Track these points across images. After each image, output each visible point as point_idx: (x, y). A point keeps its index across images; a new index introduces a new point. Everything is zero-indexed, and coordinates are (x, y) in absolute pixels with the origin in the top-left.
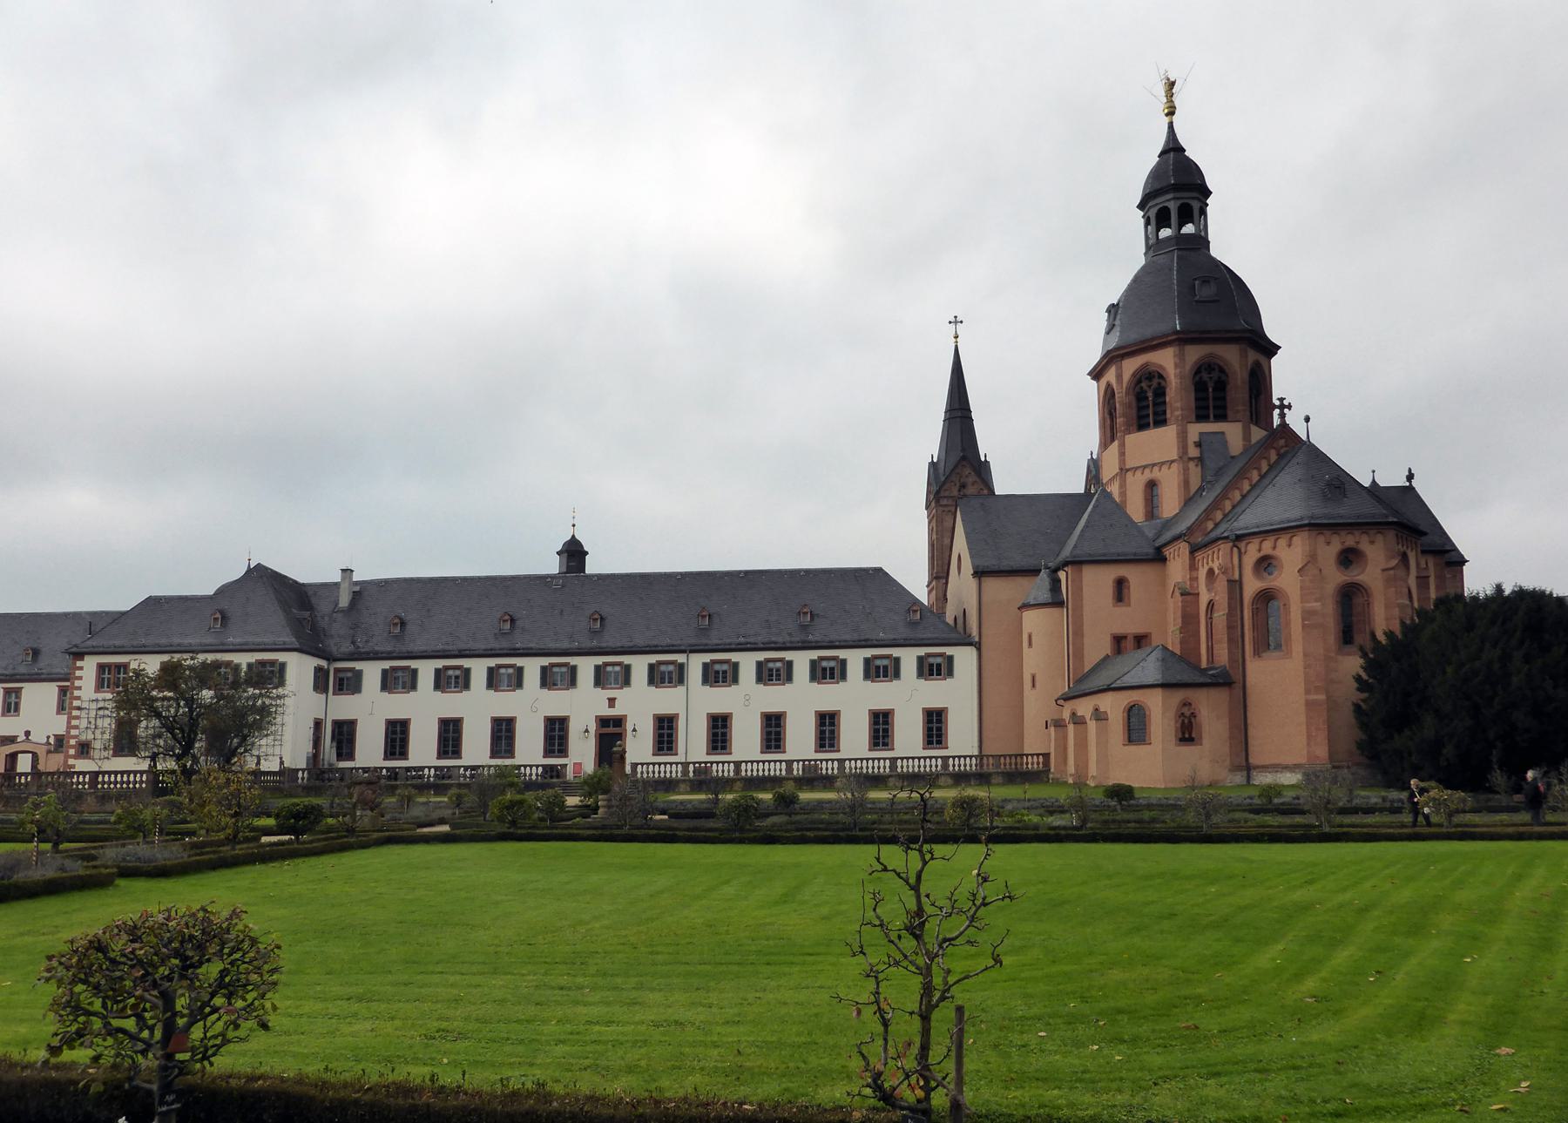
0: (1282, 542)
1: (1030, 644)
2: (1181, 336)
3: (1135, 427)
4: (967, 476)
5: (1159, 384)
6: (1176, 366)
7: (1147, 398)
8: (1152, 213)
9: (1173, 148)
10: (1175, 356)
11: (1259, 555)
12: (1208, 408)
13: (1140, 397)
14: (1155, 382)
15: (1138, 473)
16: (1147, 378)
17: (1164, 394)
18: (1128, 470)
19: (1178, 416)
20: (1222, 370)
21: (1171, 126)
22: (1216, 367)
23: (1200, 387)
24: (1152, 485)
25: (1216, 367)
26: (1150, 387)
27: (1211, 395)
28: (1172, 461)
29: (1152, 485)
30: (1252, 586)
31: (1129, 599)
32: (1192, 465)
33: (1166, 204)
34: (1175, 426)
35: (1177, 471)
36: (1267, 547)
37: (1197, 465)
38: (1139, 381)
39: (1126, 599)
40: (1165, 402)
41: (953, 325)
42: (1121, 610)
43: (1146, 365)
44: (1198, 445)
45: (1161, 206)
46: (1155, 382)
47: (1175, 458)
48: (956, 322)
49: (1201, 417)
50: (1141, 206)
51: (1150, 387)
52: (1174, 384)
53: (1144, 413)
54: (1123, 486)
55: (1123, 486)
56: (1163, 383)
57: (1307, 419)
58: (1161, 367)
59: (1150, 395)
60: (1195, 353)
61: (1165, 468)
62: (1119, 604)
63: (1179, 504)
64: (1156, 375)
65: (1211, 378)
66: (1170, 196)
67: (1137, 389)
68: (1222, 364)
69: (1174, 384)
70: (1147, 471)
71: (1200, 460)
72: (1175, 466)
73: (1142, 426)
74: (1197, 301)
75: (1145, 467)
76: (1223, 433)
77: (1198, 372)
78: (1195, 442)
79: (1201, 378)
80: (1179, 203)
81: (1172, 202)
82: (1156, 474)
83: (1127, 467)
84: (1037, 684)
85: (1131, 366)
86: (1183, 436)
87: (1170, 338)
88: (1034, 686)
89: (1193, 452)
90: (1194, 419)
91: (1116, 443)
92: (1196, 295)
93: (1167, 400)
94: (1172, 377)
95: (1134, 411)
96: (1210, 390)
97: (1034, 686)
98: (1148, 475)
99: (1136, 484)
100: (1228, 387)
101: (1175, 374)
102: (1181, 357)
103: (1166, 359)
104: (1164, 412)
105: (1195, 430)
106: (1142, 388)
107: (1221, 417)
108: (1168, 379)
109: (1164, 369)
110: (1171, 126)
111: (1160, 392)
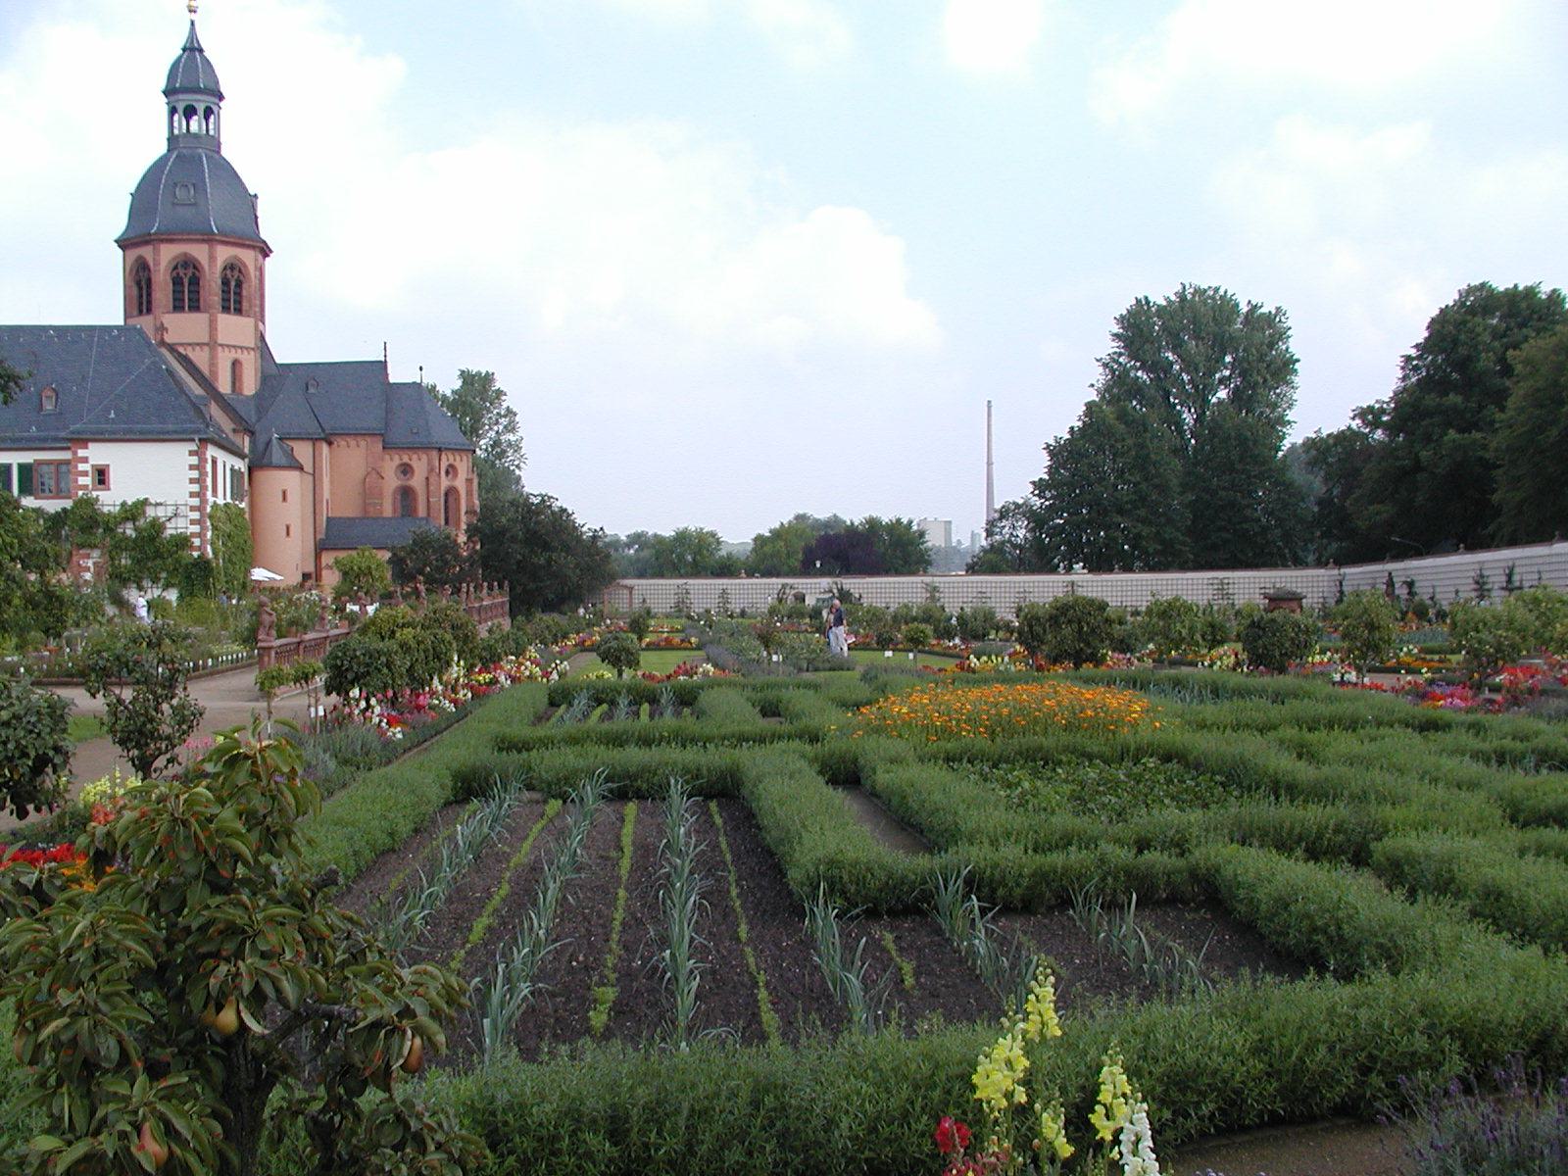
1: (284, 499)
9: (193, 48)
12: (229, 300)
13: (225, 282)
15: (226, 349)
18: (221, 345)
21: (193, 23)
24: (236, 364)
30: (445, 483)
38: (225, 269)
43: (236, 257)
46: (236, 273)
47: (253, 346)
56: (242, 278)
57: (421, 369)
58: (245, 266)
59: (233, 284)
73: (226, 309)
82: (239, 355)
83: (220, 342)
84: (291, 533)
85: (224, 254)
86: (256, 327)
88: (288, 534)
91: (200, 319)
93: (244, 293)
97: (288, 534)
110: (193, 23)
111: (239, 284)
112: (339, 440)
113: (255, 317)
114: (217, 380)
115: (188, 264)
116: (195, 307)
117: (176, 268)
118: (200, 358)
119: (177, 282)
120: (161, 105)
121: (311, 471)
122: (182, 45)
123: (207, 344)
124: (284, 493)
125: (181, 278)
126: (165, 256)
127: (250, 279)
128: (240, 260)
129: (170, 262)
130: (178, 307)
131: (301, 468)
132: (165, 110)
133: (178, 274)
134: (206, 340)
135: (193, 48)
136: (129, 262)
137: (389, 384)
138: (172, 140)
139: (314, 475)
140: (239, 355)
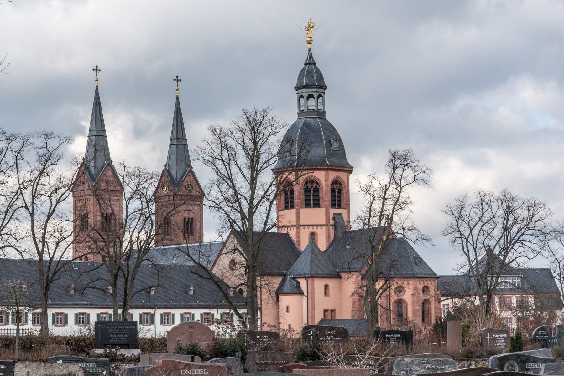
0: (405, 282)
1: (288, 311)
2: (329, 167)
3: (304, 205)
4: (109, 176)
5: (316, 187)
6: (326, 181)
7: (310, 191)
8: (305, 95)
9: (310, 62)
10: (325, 176)
11: (396, 286)
13: (307, 190)
14: (314, 185)
15: (306, 228)
16: (310, 182)
17: (318, 191)
19: (326, 205)
20: (340, 184)
21: (310, 50)
22: (339, 182)
23: (333, 191)
24: (313, 234)
25: (339, 182)
26: (312, 187)
27: (336, 195)
28: (324, 225)
29: (313, 234)
30: (394, 297)
31: (329, 293)
32: (331, 228)
33: (312, 93)
34: (324, 209)
35: (325, 231)
36: (400, 282)
37: (333, 229)
38: (307, 183)
39: (328, 294)
40: (319, 195)
41: (95, 72)
42: (327, 298)
44: (334, 219)
45: (310, 93)
46: (314, 185)
47: (324, 224)
48: (97, 70)
49: (333, 206)
50: (297, 88)
51: (312, 187)
52: (324, 189)
53: (308, 198)
54: (298, 233)
55: (298, 233)
56: (318, 187)
58: (318, 179)
60: (333, 175)
61: (319, 228)
62: (326, 296)
63: (326, 245)
64: (315, 182)
65: (336, 187)
66: (315, 90)
67: (306, 187)
68: (341, 181)
69: (324, 189)
70: (311, 228)
71: (335, 226)
72: (324, 228)
73: (307, 205)
74: (332, 150)
75: (310, 225)
76: (341, 214)
77: (332, 184)
78: (332, 218)
79: (333, 187)
80: (318, 94)
81: (315, 93)
82: (315, 230)
83: (301, 224)
86: (327, 214)
87: (324, 167)
89: (332, 222)
90: (331, 207)
91: (293, 211)
92: (331, 147)
93: (320, 195)
94: (324, 186)
95: (304, 197)
96: (336, 193)
98: (311, 230)
99: (305, 233)
100: (342, 192)
101: (325, 184)
102: (327, 176)
103: (320, 175)
104: (319, 200)
105: (333, 211)
106: (307, 187)
107: (340, 206)
108: (321, 186)
109: (319, 180)
110: (310, 50)
111: (317, 190)
112: (344, 275)
113: (326, 207)
114: (299, 244)
116: (292, 207)
118: (293, 233)
120: (294, 95)
121: (306, 295)
122: (304, 62)
123: (294, 226)
124: (288, 308)
125: (287, 191)
128: (315, 177)
130: (286, 208)
131: (302, 293)
132: (296, 97)
134: (295, 224)
135: (310, 62)
138: (301, 113)
139: (307, 297)
140: (315, 230)
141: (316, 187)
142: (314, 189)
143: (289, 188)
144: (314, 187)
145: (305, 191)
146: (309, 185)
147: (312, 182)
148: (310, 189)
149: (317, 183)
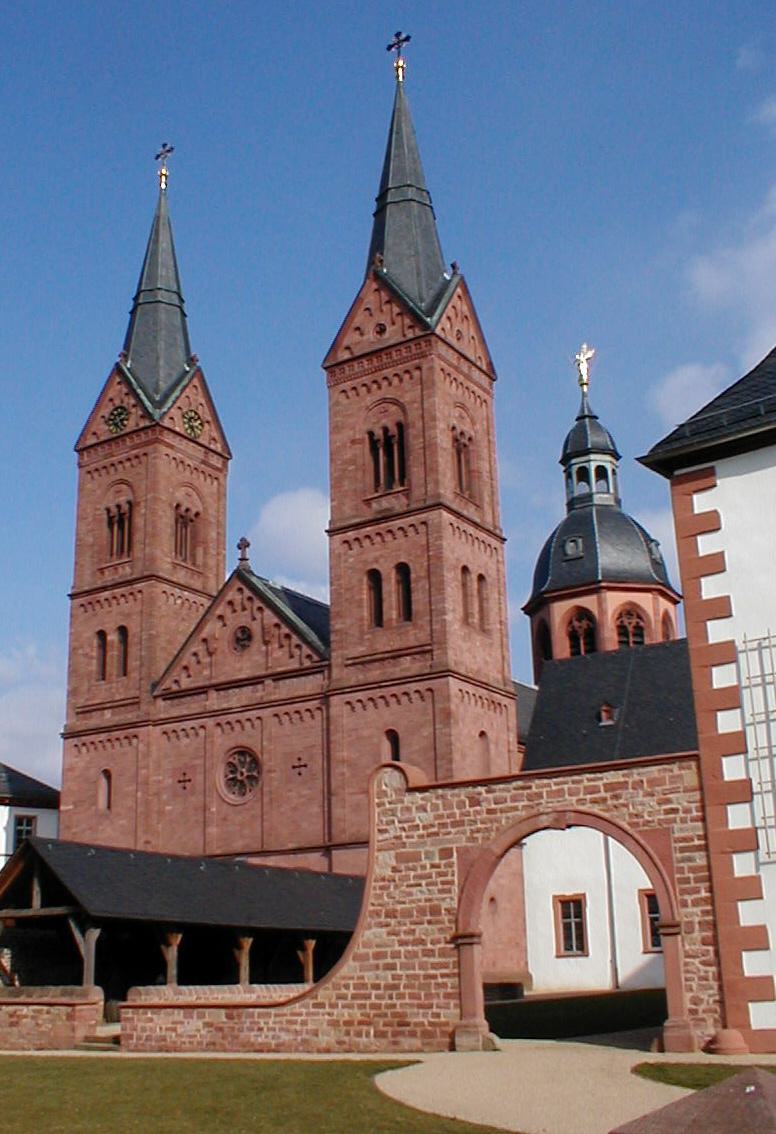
5: (637, 623)
6: (655, 614)
14: (634, 621)
17: (642, 636)
26: (630, 623)
38: (620, 616)
56: (642, 624)
59: (630, 628)
67: (618, 623)
85: (614, 601)
106: (622, 622)
109: (644, 611)
115: (583, 613)
117: (571, 622)
119: (573, 637)
125: (576, 632)
126: (560, 611)
127: (649, 626)
129: (563, 619)
133: (573, 627)
136: (536, 623)
137: (704, 622)
141: (637, 623)
142: (634, 627)
143: (580, 627)
144: (634, 624)
145: (620, 634)
146: (626, 622)
147: (629, 613)
148: (625, 627)
149: (639, 617)
